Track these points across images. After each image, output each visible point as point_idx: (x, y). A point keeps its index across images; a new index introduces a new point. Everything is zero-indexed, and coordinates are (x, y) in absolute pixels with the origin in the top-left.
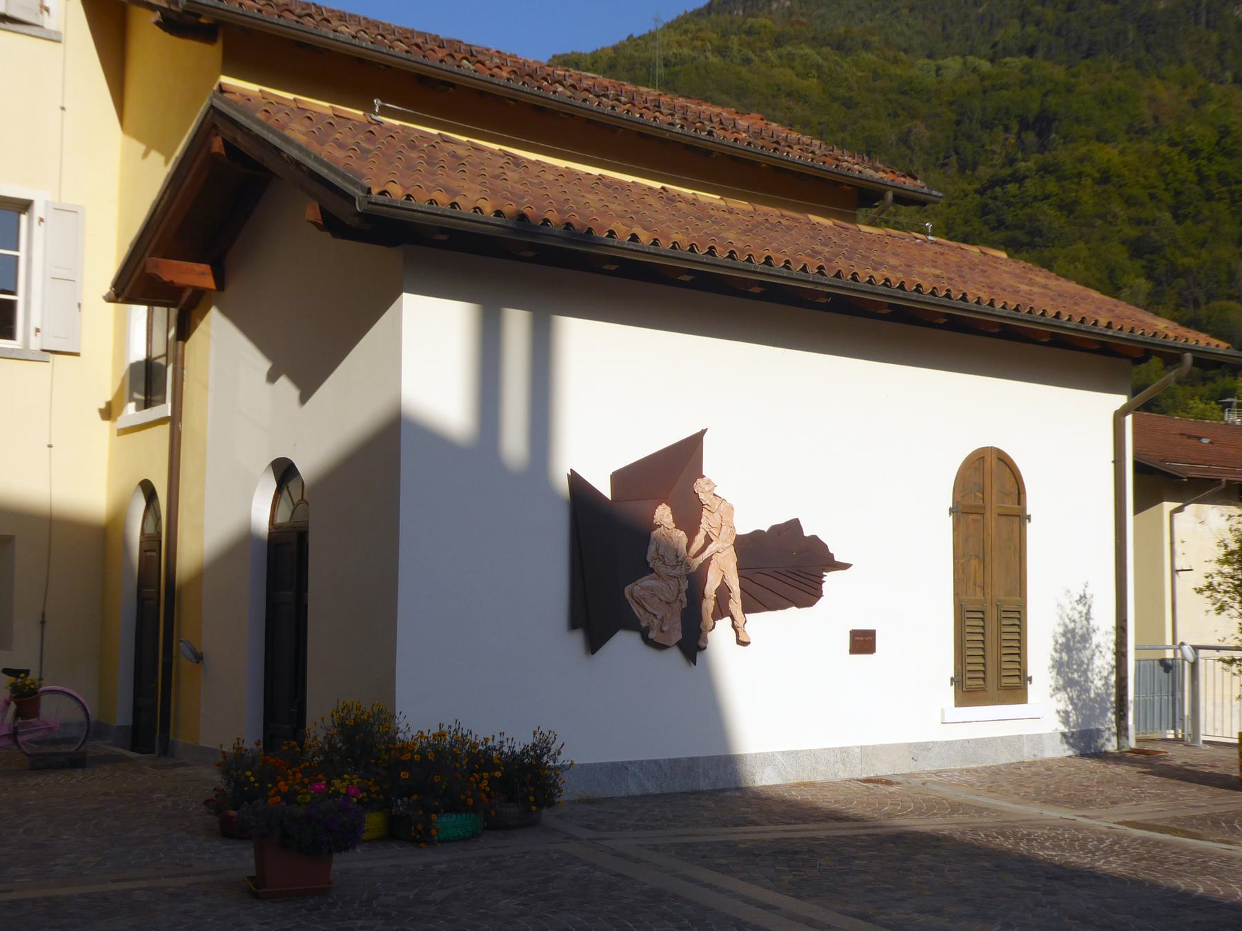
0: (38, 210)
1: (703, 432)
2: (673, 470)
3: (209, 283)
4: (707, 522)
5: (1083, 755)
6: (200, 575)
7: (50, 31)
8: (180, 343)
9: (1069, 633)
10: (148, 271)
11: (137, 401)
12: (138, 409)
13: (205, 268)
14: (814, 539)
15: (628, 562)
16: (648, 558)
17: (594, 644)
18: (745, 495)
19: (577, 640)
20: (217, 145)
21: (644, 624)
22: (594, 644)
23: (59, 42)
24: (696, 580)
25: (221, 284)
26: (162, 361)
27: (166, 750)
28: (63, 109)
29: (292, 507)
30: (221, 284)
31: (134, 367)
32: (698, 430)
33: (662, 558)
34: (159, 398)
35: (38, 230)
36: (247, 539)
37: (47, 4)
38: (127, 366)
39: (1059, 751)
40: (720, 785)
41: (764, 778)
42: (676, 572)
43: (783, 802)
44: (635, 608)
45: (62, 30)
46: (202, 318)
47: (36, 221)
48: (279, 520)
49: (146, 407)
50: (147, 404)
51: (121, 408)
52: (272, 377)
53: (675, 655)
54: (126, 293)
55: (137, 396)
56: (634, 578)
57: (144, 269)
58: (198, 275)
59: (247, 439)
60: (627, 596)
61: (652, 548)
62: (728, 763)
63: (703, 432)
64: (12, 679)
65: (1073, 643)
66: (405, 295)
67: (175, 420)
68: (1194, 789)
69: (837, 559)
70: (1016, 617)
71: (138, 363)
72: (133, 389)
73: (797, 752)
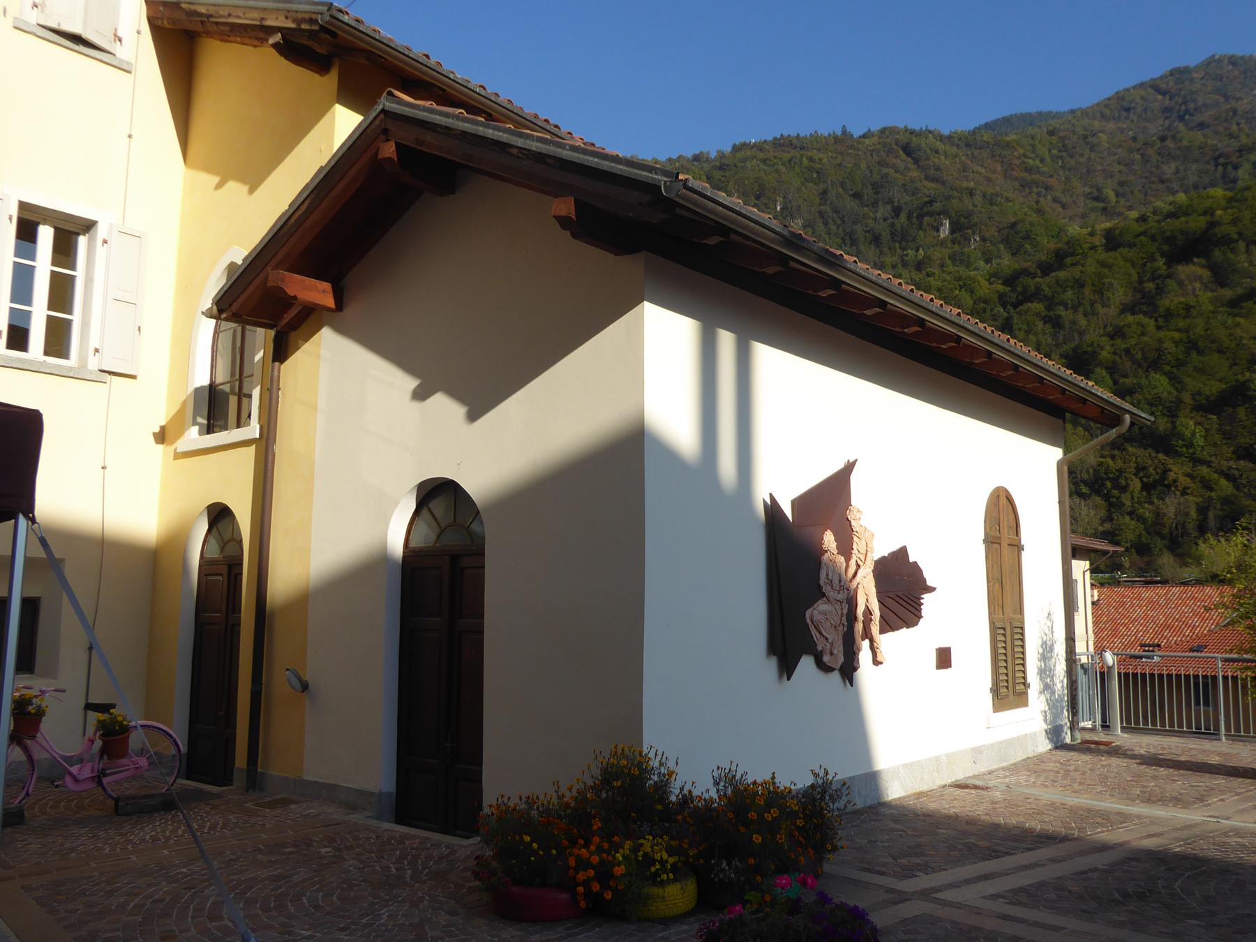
0: (101, 231)
1: (850, 467)
2: (831, 497)
3: (329, 302)
4: (858, 546)
5: (1056, 748)
6: (302, 601)
7: (121, 60)
8: (277, 364)
9: (1044, 643)
10: (270, 284)
11: (200, 425)
12: (201, 433)
13: (327, 286)
14: (915, 563)
15: (810, 591)
16: (822, 583)
17: (787, 668)
18: (881, 524)
19: (772, 664)
20: (389, 150)
21: (820, 648)
22: (787, 668)
23: (130, 72)
24: (852, 602)
25: (340, 305)
26: (227, 388)
27: (254, 781)
28: (130, 136)
29: (438, 531)
30: (340, 305)
31: (198, 391)
32: (840, 465)
33: (831, 583)
34: (221, 423)
35: (100, 250)
36: (382, 559)
37: (119, 34)
38: (191, 390)
39: (1044, 746)
40: (869, 803)
41: (895, 790)
42: (840, 596)
43: (951, 821)
44: (813, 631)
45: (133, 61)
46: (306, 340)
47: (99, 241)
48: (413, 544)
49: (208, 433)
50: (209, 429)
51: (180, 432)
52: (420, 395)
53: (836, 676)
54: (235, 306)
55: (200, 420)
56: (811, 603)
57: (266, 280)
58: (319, 293)
59: (363, 457)
60: (808, 620)
61: (823, 573)
62: (872, 779)
63: (850, 467)
64: (101, 717)
65: (1047, 652)
66: (646, 303)
67: (265, 446)
68: (1163, 771)
69: (929, 583)
70: (1019, 631)
71: (202, 388)
72: (196, 413)
73: (912, 764)
